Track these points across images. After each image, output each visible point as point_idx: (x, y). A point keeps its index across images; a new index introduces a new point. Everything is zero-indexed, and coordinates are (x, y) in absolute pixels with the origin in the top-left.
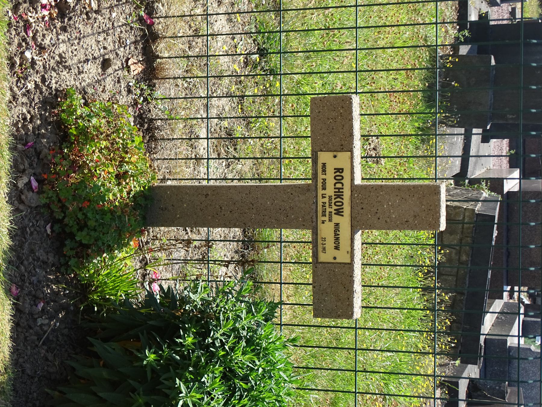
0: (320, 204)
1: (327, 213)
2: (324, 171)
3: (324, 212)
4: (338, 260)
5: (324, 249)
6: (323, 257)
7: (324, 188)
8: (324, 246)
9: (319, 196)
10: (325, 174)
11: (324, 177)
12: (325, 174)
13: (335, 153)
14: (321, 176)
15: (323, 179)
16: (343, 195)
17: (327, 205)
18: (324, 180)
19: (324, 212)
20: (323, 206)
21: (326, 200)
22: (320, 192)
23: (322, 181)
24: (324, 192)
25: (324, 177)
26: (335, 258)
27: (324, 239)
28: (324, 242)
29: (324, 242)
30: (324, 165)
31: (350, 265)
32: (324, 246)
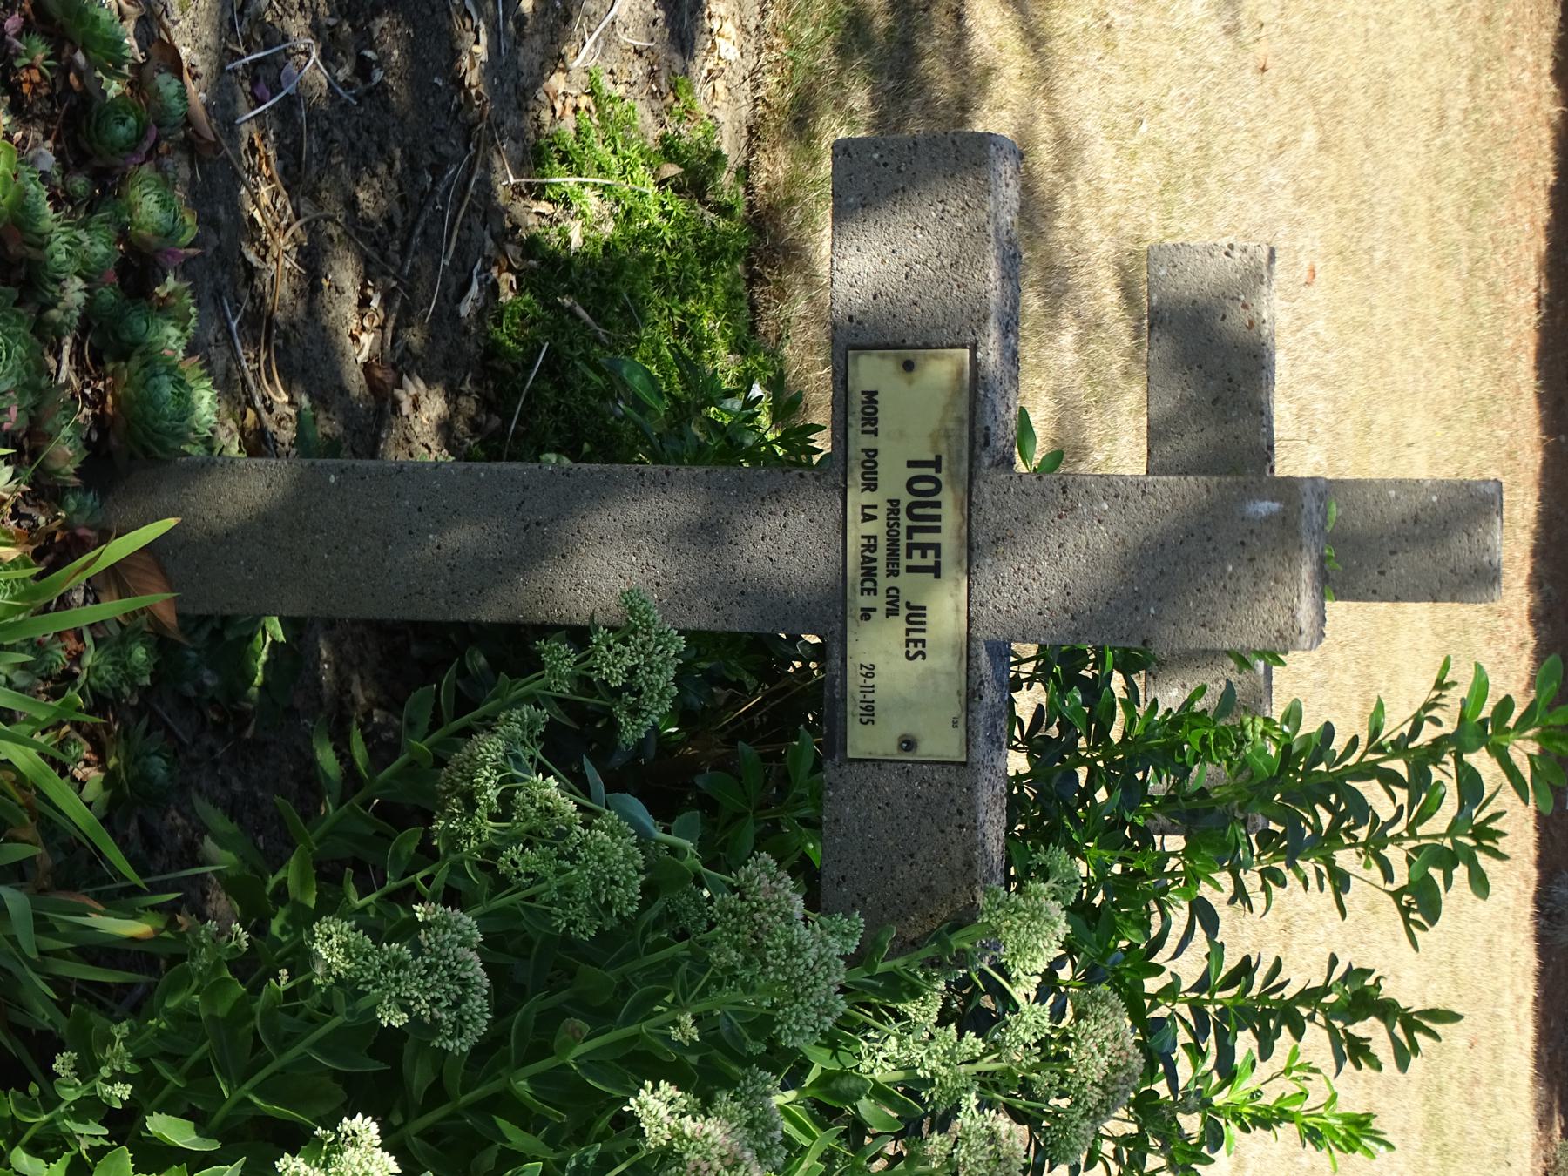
2: (871, 420)
5: (869, 708)
7: (871, 486)
8: (870, 697)
11: (867, 442)
12: (875, 433)
13: (909, 354)
14: (859, 441)
18: (872, 454)
19: (869, 573)
20: (867, 548)
21: (877, 528)
23: (863, 456)
25: (867, 442)
26: (908, 743)
29: (870, 682)
30: (871, 397)
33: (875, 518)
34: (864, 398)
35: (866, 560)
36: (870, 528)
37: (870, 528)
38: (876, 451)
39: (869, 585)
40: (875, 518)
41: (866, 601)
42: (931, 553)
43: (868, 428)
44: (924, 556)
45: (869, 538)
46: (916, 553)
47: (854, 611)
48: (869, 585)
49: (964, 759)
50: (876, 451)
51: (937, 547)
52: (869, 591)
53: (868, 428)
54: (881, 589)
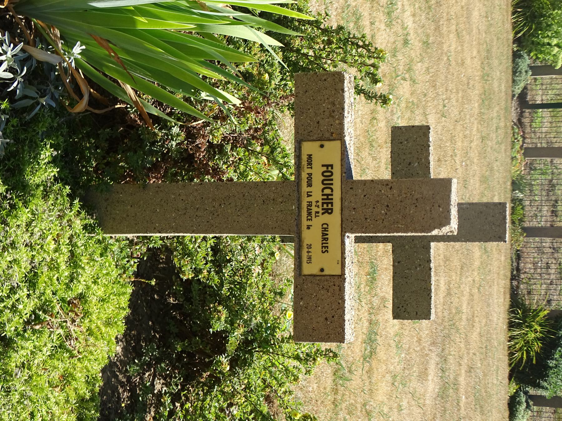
0: (304, 205)
1: (313, 215)
2: (310, 163)
3: (309, 214)
4: (326, 272)
5: (310, 258)
6: (308, 269)
7: (310, 185)
9: (304, 195)
10: (311, 168)
11: (309, 171)
12: (311, 168)
13: (323, 143)
16: (332, 199)
17: (314, 204)
18: (310, 175)
20: (309, 205)
22: (305, 188)
24: (309, 189)
25: (309, 171)
26: (322, 270)
27: (309, 246)
28: (310, 250)
29: (310, 250)
30: (310, 156)
31: (341, 277)
32: (310, 254)
33: (311, 196)
34: (307, 157)
35: (308, 209)
36: (309, 199)
37: (309, 199)
38: (311, 174)
39: (309, 218)
40: (311, 196)
41: (309, 223)
42: (330, 205)
43: (309, 166)
44: (327, 206)
45: (309, 202)
46: (325, 206)
47: (304, 227)
48: (309, 218)
49: (340, 274)
50: (311, 174)
51: (332, 203)
52: (309, 219)
53: (309, 166)
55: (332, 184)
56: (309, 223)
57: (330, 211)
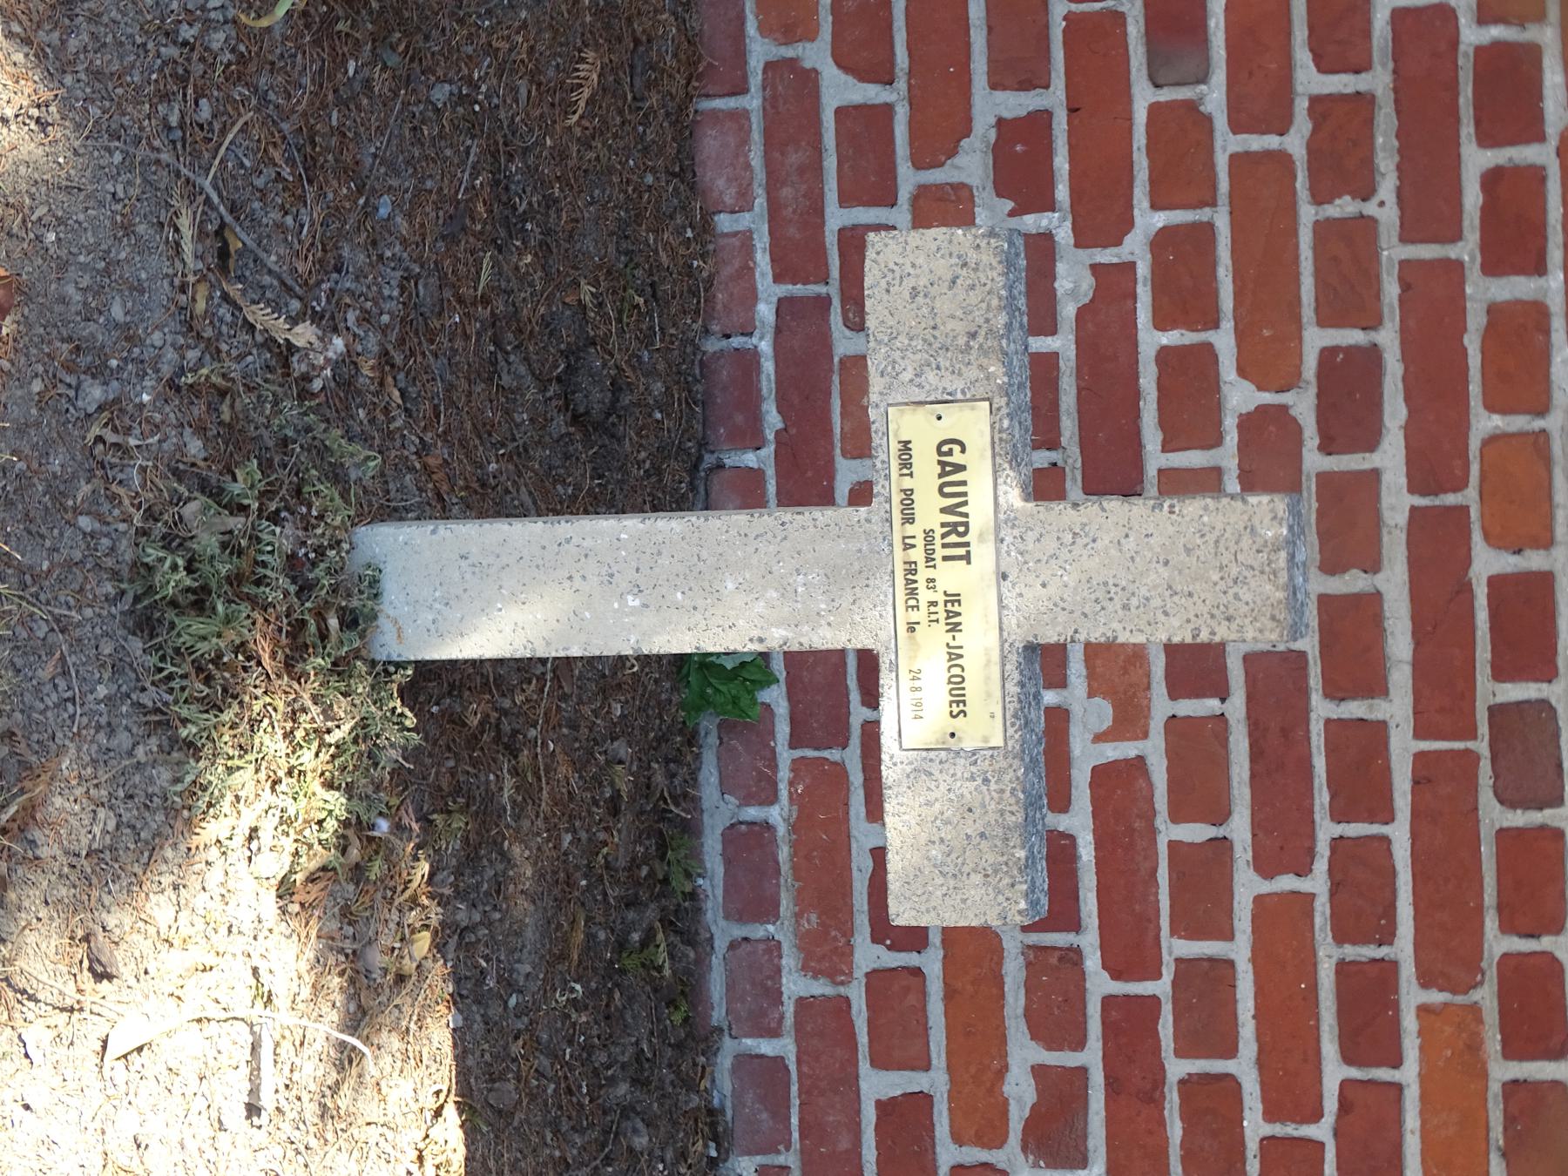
2: (906, 464)
5: (918, 704)
7: (909, 519)
10: (911, 475)
11: (907, 483)
12: (911, 475)
14: (897, 482)
15: (904, 491)
18: (908, 493)
19: (912, 593)
21: (918, 554)
24: (910, 530)
25: (907, 483)
28: (917, 684)
29: (917, 684)
34: (900, 446)
35: (909, 582)
41: (914, 616)
53: (905, 471)
54: (923, 605)
55: (964, 483)
56: (914, 616)
57: (961, 529)
